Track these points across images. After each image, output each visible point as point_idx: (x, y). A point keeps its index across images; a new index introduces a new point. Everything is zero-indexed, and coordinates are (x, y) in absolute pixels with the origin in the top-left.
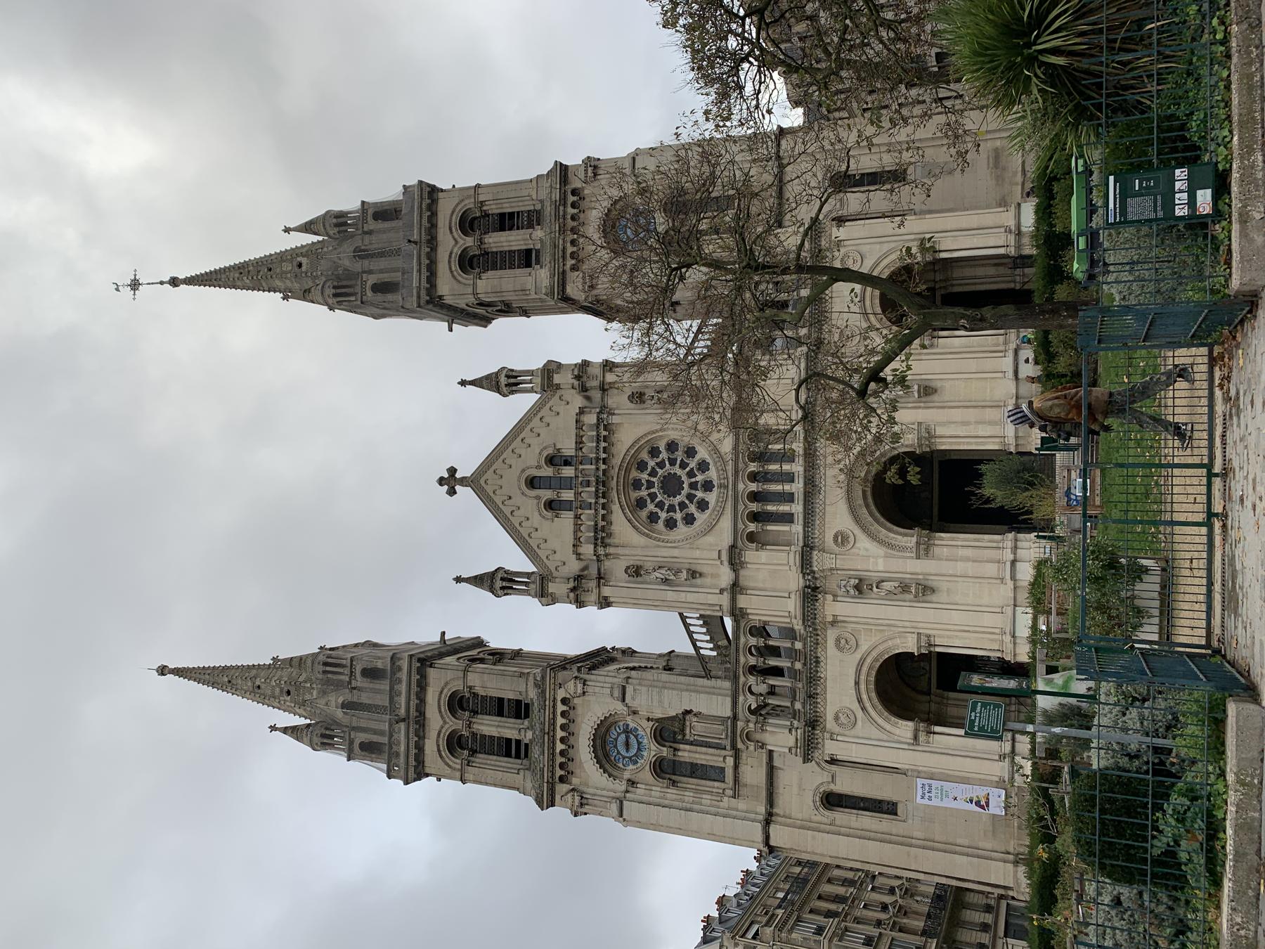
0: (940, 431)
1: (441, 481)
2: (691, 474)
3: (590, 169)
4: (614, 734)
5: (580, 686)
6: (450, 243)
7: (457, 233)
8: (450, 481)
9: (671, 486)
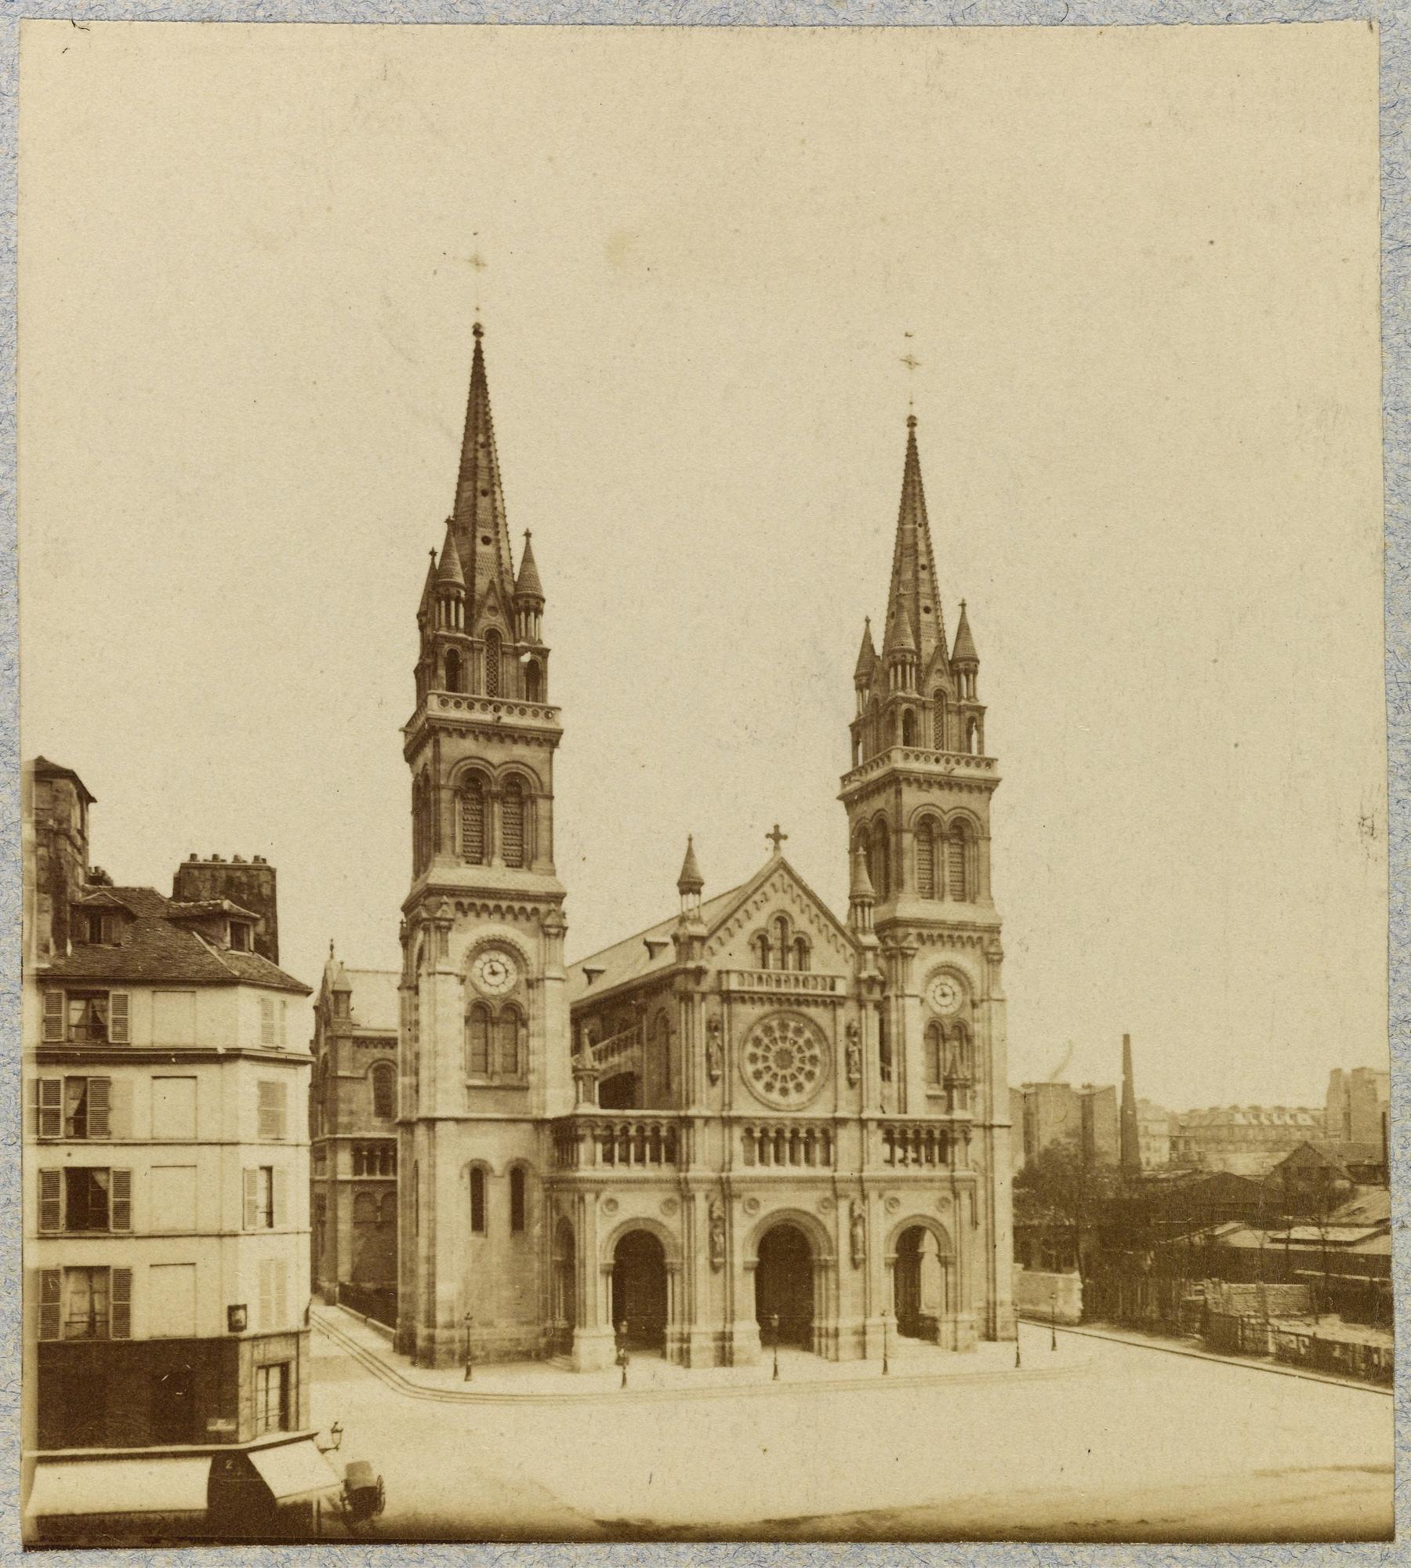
0: (832, 1275)
1: (777, 827)
2: (793, 1077)
3: (996, 957)
4: (503, 958)
5: (553, 931)
6: (944, 801)
7: (952, 816)
8: (777, 836)
9: (785, 1058)
